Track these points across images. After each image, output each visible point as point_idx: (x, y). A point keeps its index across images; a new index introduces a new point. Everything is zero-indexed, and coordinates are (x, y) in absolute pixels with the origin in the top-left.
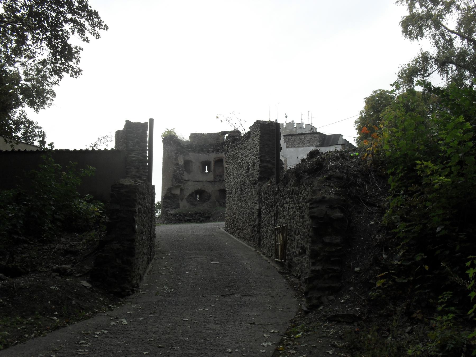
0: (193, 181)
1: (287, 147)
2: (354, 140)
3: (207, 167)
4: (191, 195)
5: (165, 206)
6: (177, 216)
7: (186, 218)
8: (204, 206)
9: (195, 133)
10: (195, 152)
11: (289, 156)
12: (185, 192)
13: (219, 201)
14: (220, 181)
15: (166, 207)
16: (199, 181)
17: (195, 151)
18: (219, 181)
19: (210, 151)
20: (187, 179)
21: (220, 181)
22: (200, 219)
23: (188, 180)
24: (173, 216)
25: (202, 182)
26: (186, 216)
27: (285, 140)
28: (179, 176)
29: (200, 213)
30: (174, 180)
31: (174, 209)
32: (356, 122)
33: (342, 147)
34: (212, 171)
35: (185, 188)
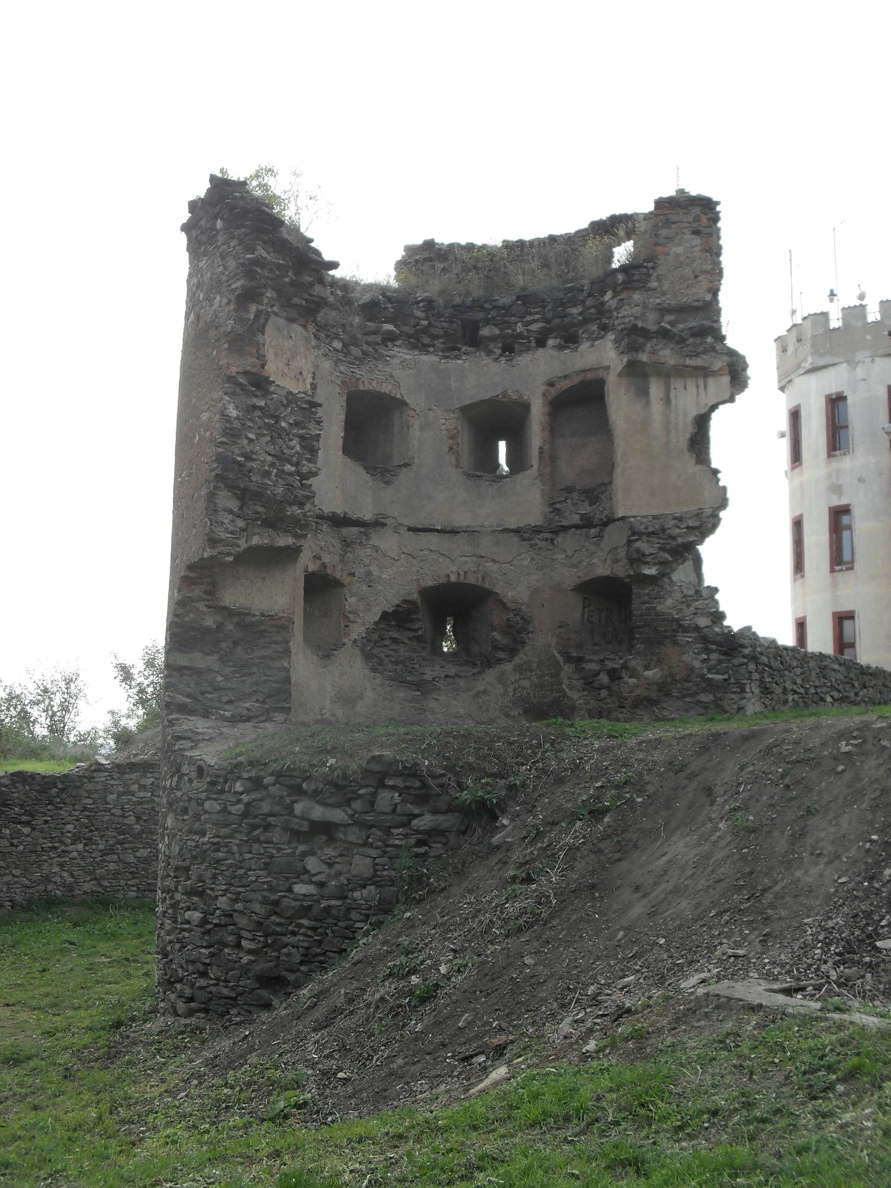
0: (410, 529)
3: (502, 446)
5: (181, 699)
7: (299, 808)
8: (485, 692)
9: (429, 245)
10: (424, 348)
12: (352, 600)
13: (580, 660)
14: (587, 523)
15: (183, 709)
16: (453, 532)
17: (426, 340)
18: (577, 527)
19: (520, 336)
20: (368, 515)
21: (587, 523)
22: (414, 822)
23: (378, 524)
24: (213, 783)
25: (471, 532)
26: (298, 791)
28: (267, 474)
29: (412, 772)
30: (227, 501)
31: (249, 719)
34: (535, 460)
35: (353, 574)
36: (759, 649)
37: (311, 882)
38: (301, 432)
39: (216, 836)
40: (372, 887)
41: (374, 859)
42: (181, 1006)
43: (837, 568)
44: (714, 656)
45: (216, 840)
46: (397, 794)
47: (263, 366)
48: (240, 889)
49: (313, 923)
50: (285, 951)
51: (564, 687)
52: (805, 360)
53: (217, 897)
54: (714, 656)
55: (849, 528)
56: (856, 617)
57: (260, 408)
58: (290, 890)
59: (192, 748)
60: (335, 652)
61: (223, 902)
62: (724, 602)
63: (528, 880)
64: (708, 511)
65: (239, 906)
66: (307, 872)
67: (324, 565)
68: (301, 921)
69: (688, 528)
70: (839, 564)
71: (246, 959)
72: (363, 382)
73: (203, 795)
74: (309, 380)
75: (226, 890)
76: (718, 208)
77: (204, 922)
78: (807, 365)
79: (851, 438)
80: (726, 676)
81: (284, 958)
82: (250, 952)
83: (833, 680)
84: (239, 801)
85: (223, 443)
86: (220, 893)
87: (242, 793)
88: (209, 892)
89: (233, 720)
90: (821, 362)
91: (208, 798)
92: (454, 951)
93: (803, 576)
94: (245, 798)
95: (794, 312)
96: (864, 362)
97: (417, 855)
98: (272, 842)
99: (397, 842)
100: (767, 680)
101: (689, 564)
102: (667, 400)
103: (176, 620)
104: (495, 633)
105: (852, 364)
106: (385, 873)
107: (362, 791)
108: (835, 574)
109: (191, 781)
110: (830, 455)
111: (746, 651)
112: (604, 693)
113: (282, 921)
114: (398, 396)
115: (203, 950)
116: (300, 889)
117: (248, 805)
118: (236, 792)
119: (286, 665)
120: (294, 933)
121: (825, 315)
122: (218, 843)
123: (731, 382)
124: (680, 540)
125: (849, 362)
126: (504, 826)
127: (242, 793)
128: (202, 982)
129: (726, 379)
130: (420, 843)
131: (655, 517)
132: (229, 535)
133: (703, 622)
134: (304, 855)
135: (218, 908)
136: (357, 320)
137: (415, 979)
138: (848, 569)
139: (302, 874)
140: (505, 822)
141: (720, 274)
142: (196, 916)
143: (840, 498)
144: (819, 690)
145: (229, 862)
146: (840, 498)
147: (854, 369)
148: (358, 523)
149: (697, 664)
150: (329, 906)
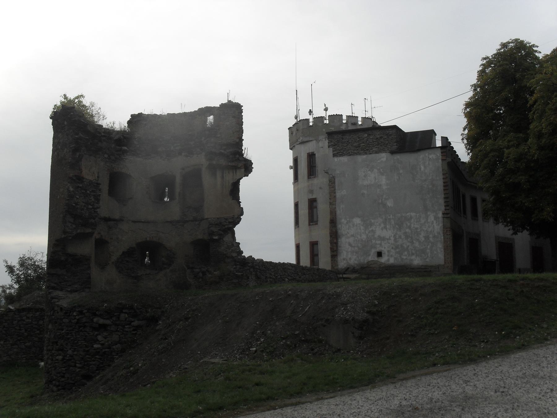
1: (334, 155)
2: (463, 139)
4: (129, 253)
5: (53, 285)
6: (75, 314)
7: (95, 320)
11: (338, 172)
15: (54, 288)
20: (117, 217)
22: (132, 323)
23: (121, 220)
24: (66, 313)
26: (95, 315)
27: (331, 142)
31: (76, 291)
32: (468, 105)
33: (442, 153)
36: (255, 264)
37: (99, 344)
38: (94, 194)
39: (67, 330)
40: (119, 345)
41: (120, 335)
42: (55, 389)
43: (311, 224)
44: (238, 267)
45: (67, 332)
46: (126, 315)
47: (81, 173)
48: (76, 347)
49: (100, 357)
50: (91, 366)
51: (187, 277)
52: (299, 138)
53: (68, 351)
54: (238, 267)
55: (316, 207)
56: (319, 244)
57: (80, 187)
58: (93, 347)
59: (58, 301)
60: (105, 266)
61: (70, 352)
62: (242, 247)
63: (166, 339)
64: (236, 216)
65: (75, 353)
66: (98, 340)
67: (102, 236)
68: (96, 357)
69: (229, 222)
70: (312, 222)
71: (78, 370)
72: (115, 169)
73: (63, 317)
74: (97, 175)
75: (70, 348)
76: (242, 108)
77: (63, 359)
78: (300, 140)
79: (317, 171)
80: (242, 274)
81: (90, 369)
82: (79, 368)
83: (289, 273)
84: (75, 319)
85: (68, 200)
86: (69, 349)
87: (76, 316)
88: (65, 349)
89: (71, 292)
90: (305, 139)
91: (64, 318)
92: (143, 360)
93: (298, 227)
94: (77, 317)
95: (296, 118)
96: (322, 140)
97: (133, 334)
98: (86, 331)
99: (127, 330)
100: (259, 274)
101: (230, 235)
102: (223, 177)
103: (51, 258)
104: (163, 259)
105: (318, 141)
106: (123, 340)
107: (116, 314)
108: (310, 226)
109: (58, 312)
110: (309, 178)
111: (250, 265)
112: (200, 280)
113: (90, 357)
114: (128, 173)
115: (63, 369)
116: (96, 346)
117: (78, 319)
118: (74, 316)
119: (89, 272)
120: (94, 361)
121: (307, 120)
122: (68, 333)
123: (245, 170)
124: (226, 227)
125: (316, 140)
126: (160, 324)
127: (76, 316)
128: (63, 379)
129: (243, 170)
130: (134, 330)
131: (218, 218)
132: (70, 230)
133: (234, 255)
134: (97, 335)
135: (68, 354)
136: (113, 146)
137: (131, 369)
138: (315, 224)
139: (96, 341)
140: (160, 322)
141: (242, 132)
142: (60, 357)
143: (312, 195)
144: (282, 277)
145: (72, 338)
146: (312, 195)
147: (318, 143)
148: (114, 220)
149: (232, 269)
150: (105, 351)
